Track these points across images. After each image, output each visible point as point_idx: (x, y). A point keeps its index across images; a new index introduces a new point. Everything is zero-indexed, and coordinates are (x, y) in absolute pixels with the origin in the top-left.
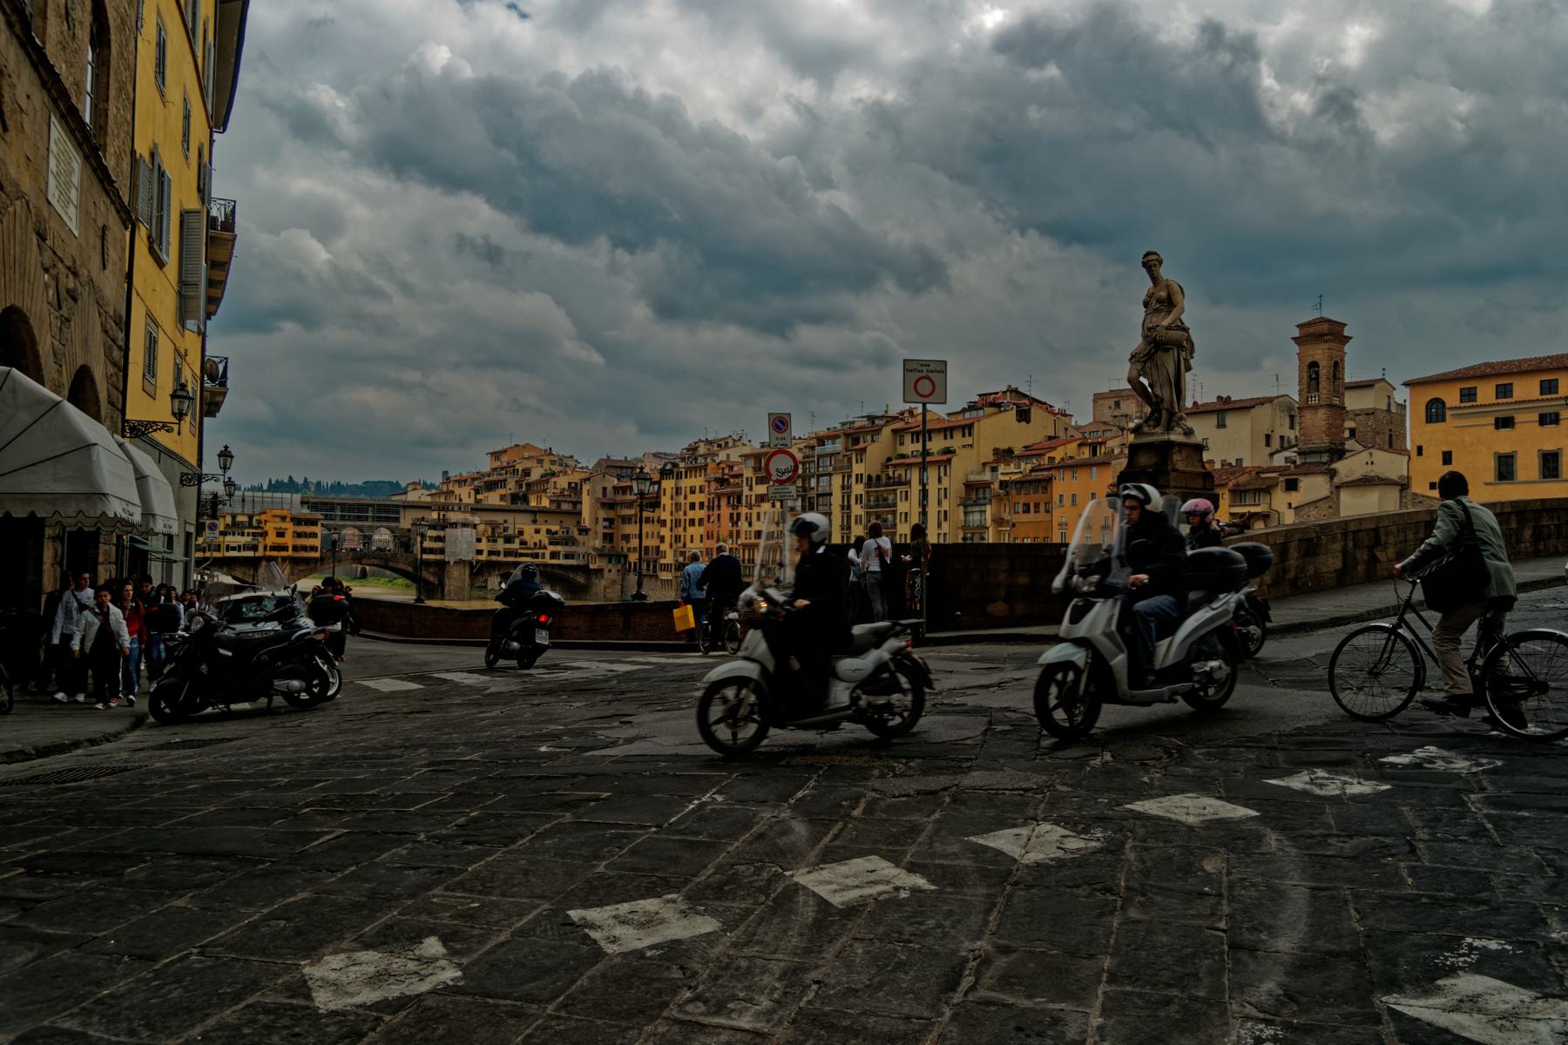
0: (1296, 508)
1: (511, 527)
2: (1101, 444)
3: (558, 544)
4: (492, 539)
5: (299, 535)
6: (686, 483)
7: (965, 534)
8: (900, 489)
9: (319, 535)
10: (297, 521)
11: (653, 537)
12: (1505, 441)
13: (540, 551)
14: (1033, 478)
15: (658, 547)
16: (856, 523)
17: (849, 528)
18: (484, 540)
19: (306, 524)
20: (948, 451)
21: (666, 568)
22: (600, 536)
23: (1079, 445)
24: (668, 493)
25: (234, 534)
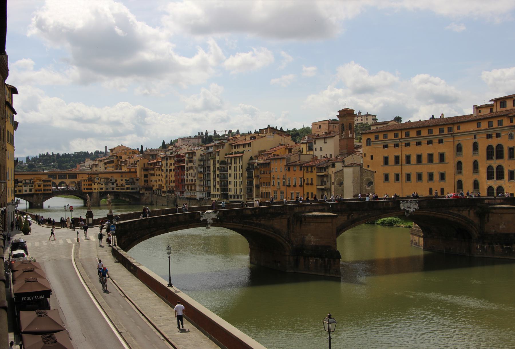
0: (334, 173)
1: (113, 179)
2: (292, 148)
3: (129, 184)
4: (106, 184)
6: (169, 162)
7: (248, 181)
8: (229, 166)
11: (160, 181)
12: (386, 152)
14: (266, 162)
15: (162, 185)
16: (217, 177)
17: (215, 179)
19: (47, 182)
20: (243, 152)
21: (164, 192)
22: (143, 181)
23: (286, 149)
24: (164, 166)
25: (26, 187)
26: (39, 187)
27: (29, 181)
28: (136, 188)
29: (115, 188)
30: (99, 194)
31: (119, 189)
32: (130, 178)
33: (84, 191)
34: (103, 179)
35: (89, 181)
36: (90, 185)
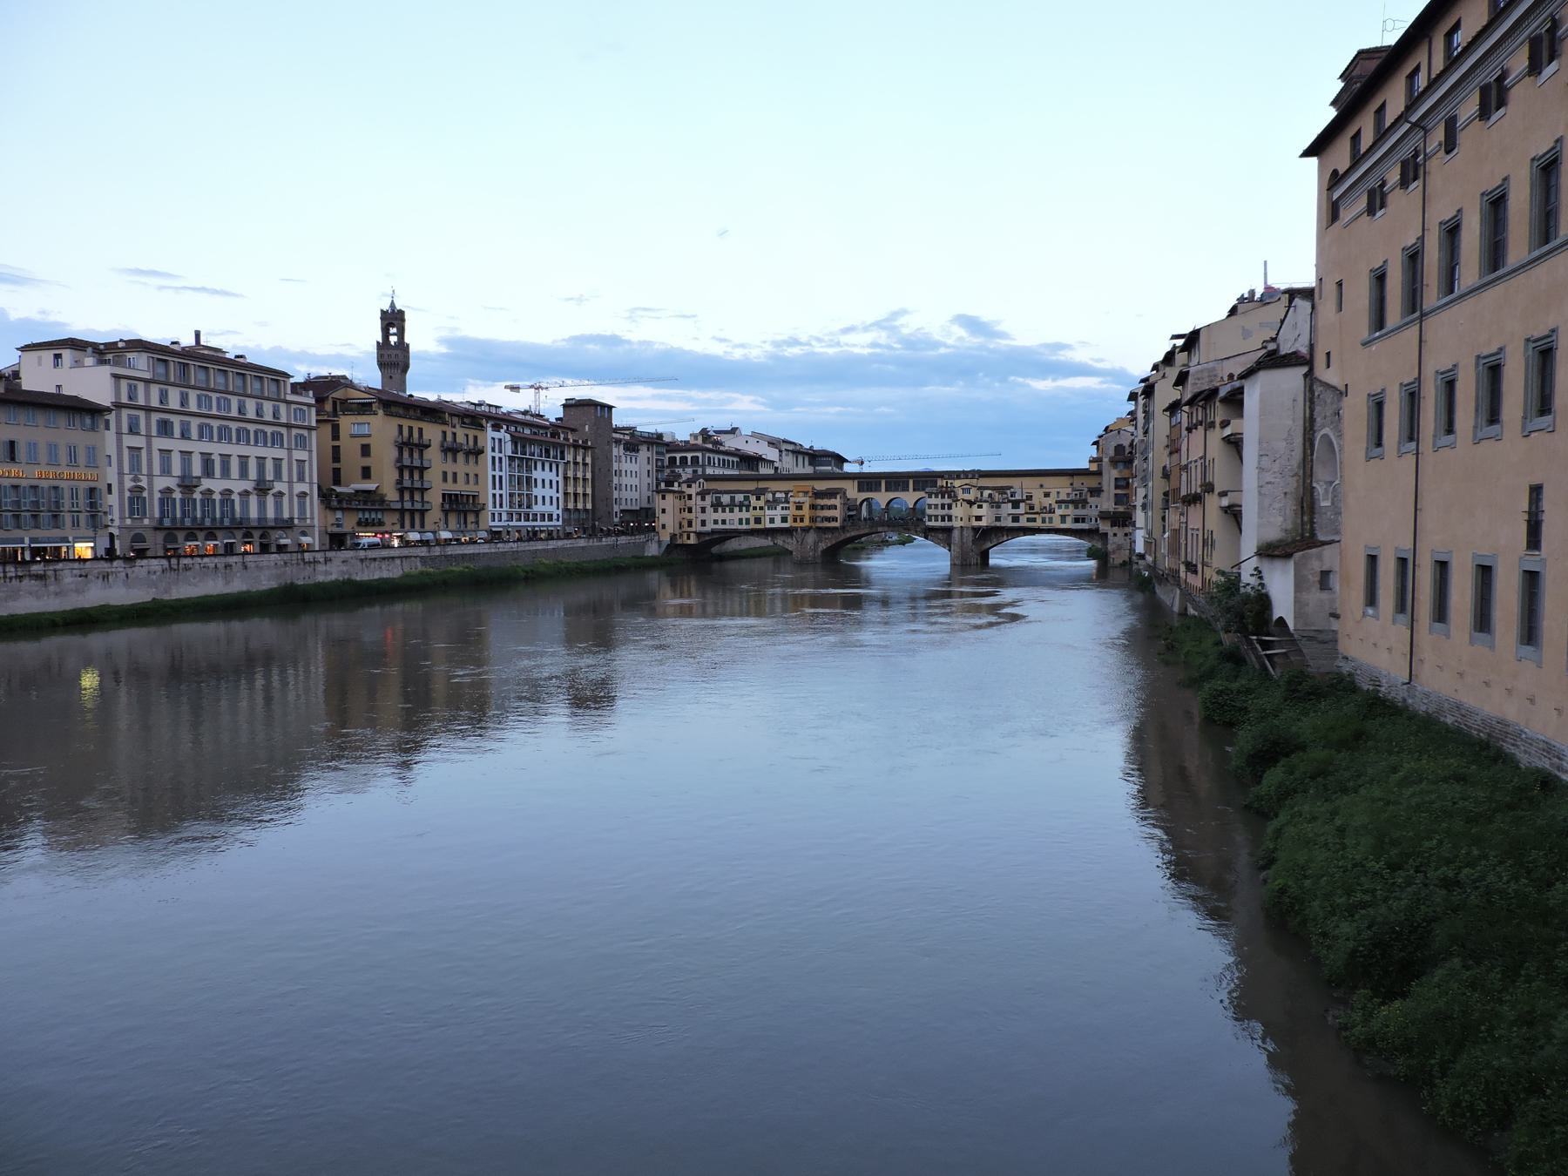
1: (1019, 491)
5: (823, 508)
10: (818, 494)
13: (1047, 516)
18: (985, 505)
27: (784, 496)
28: (1091, 519)
29: (1021, 517)
30: (969, 535)
31: (1034, 520)
32: (1074, 490)
33: (928, 523)
34: (990, 492)
35: (943, 497)
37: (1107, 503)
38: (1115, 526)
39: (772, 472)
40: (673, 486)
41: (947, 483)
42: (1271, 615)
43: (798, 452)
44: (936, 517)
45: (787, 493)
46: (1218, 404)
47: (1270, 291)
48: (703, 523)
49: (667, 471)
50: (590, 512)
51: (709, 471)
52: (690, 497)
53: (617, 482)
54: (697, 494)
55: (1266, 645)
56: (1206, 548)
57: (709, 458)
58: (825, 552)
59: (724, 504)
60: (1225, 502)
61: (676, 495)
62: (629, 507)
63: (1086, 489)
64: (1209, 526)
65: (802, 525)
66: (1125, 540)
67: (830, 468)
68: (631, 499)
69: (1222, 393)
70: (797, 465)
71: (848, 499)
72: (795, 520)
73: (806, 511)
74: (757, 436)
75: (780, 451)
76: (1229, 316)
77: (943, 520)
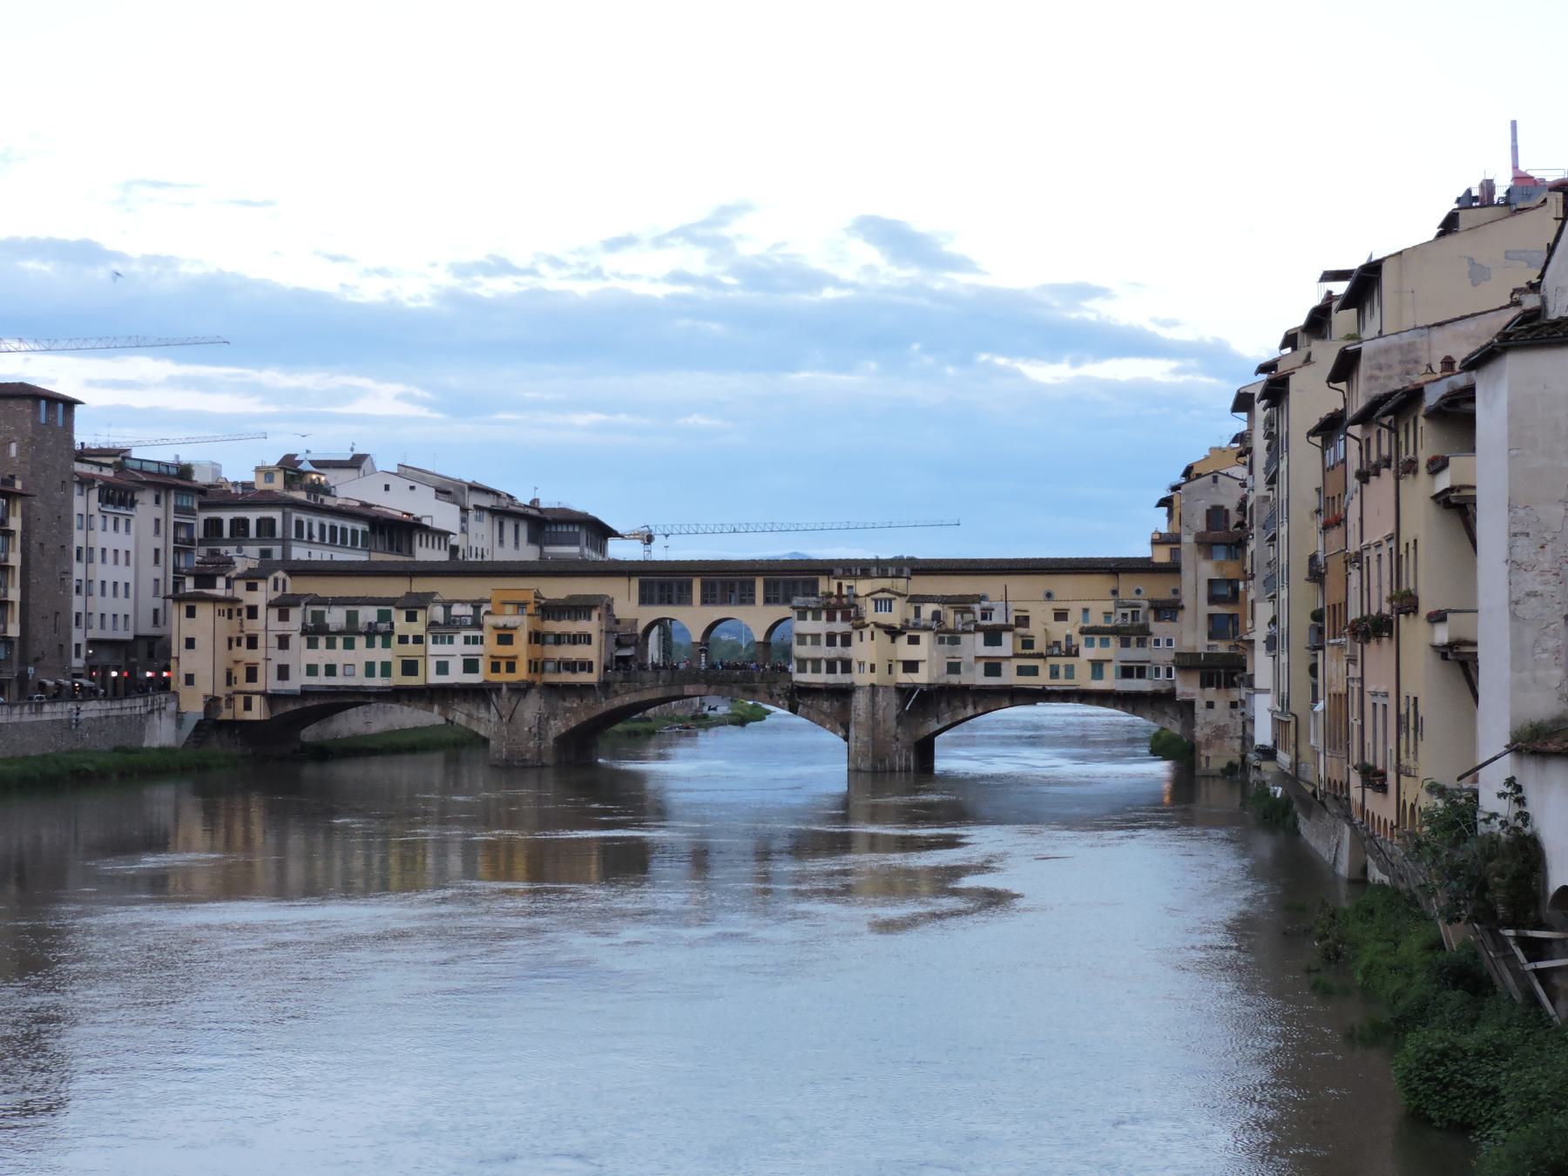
4: (951, 637)
5: (559, 639)
9: (595, 639)
10: (549, 610)
13: (1062, 662)
18: (925, 637)
25: (443, 642)
26: (501, 647)
27: (469, 610)
28: (1157, 670)
29: (1005, 665)
31: (1034, 671)
35: (831, 618)
36: (839, 639)
37: (1191, 634)
38: (1210, 684)
39: (442, 556)
40: (214, 586)
41: (840, 586)
42: (1544, 882)
43: (504, 512)
44: (816, 663)
45: (477, 605)
46: (1422, 421)
47: (1524, 183)
48: (283, 672)
49: (200, 552)
50: (16, 646)
51: (299, 553)
52: (252, 612)
53: (82, 577)
54: (270, 605)
55: (1536, 950)
56: (1403, 736)
57: (299, 524)
58: (560, 740)
59: (332, 629)
60: (1442, 635)
61: (224, 607)
62: (108, 634)
63: (1146, 604)
64: (1408, 688)
65: (511, 678)
66: (1231, 716)
67: (575, 550)
68: (115, 616)
69: (1432, 397)
70: (501, 542)
71: (618, 622)
72: (495, 668)
73: (520, 648)
74: (411, 475)
75: (464, 510)
76: (1440, 235)
77: (831, 669)
